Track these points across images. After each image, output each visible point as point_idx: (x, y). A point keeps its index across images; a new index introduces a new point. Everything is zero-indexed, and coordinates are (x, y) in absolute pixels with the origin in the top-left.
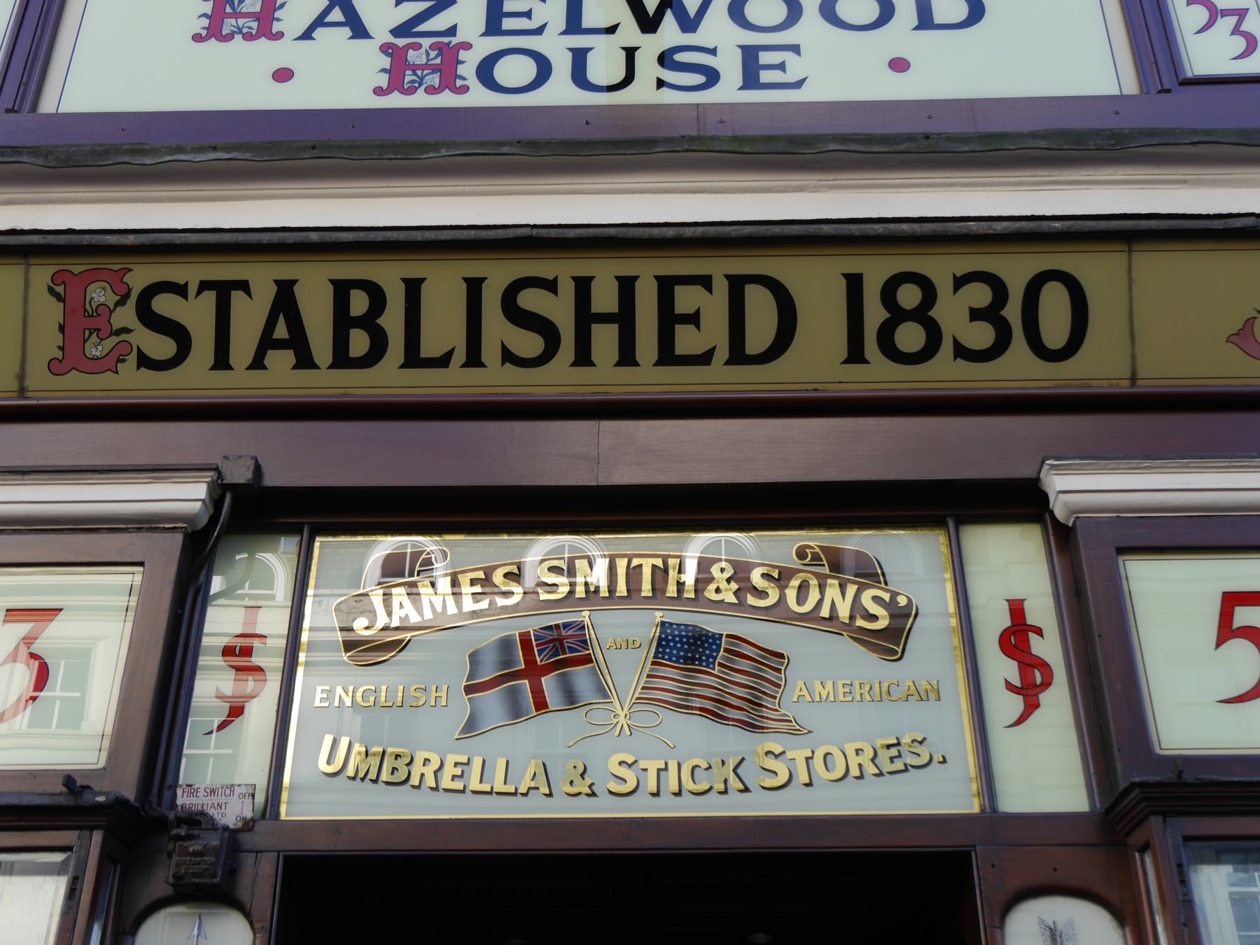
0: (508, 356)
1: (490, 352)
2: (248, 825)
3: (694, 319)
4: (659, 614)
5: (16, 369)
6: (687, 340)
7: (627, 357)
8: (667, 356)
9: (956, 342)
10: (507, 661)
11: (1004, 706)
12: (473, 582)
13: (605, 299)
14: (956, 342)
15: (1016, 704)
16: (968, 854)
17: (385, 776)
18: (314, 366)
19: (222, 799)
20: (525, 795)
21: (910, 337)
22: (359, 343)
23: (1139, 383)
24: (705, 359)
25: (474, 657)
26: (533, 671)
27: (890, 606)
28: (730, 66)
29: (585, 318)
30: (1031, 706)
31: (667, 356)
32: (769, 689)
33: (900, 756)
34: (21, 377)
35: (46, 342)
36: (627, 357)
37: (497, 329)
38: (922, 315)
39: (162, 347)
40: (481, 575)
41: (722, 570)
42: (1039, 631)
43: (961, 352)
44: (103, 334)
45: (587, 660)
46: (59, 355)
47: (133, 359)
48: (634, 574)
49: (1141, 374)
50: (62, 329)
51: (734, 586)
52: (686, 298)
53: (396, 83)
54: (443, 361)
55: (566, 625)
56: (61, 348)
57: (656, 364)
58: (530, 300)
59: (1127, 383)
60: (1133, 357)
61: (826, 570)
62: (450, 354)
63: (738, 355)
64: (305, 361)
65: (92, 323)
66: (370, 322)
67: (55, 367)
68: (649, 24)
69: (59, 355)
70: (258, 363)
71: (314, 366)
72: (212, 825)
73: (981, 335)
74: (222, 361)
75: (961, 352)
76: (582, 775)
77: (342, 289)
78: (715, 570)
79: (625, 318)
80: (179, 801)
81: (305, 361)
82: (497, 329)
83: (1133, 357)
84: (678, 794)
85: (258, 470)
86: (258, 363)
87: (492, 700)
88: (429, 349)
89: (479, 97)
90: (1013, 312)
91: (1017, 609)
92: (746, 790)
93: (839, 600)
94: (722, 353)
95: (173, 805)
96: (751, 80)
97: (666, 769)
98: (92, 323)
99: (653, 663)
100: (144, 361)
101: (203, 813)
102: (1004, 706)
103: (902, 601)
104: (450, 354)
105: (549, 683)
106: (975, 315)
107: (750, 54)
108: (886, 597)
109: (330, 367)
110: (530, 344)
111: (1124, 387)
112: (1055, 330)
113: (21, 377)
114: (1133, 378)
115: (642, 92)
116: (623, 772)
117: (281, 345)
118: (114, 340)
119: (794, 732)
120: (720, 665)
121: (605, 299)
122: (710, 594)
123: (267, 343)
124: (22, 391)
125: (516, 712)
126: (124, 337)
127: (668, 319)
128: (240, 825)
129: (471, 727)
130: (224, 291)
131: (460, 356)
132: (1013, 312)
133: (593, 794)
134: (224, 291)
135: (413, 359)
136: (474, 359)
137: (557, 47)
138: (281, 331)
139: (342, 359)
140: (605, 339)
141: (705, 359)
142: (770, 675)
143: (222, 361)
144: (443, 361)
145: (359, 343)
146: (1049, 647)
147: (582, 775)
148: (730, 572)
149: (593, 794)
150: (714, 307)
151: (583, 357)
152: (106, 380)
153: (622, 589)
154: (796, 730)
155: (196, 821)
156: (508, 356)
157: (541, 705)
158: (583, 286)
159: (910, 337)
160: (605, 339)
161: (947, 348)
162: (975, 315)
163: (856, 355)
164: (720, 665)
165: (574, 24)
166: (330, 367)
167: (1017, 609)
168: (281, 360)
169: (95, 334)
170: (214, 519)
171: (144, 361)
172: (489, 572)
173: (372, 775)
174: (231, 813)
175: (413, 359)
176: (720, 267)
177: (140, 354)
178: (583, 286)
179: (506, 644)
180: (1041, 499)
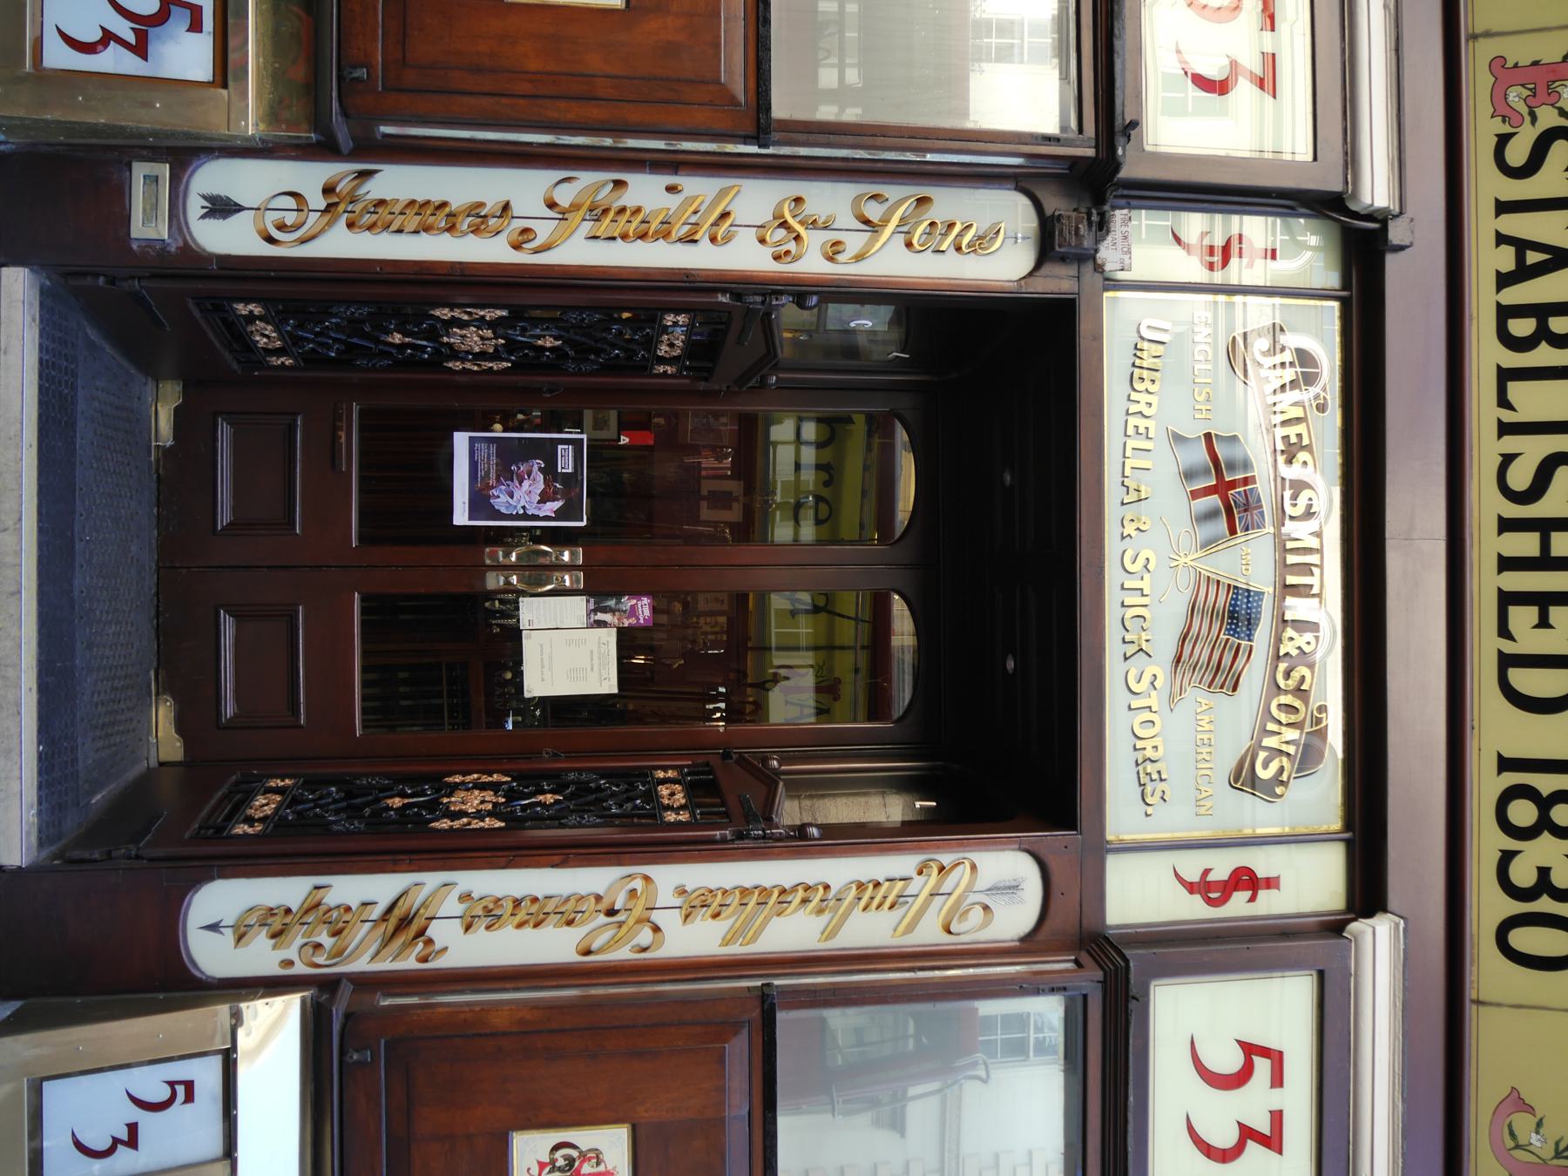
0: (1508, 459)
1: (1512, 443)
2: (1099, 268)
3: (1544, 623)
4: (1271, 590)
5: (1495, 29)
6: (1523, 617)
7: (1507, 564)
8: (1507, 599)
9: (1516, 853)
10: (1232, 466)
11: (1192, 865)
12: (1299, 436)
14: (1516, 853)
15: (1194, 876)
16: (1075, 829)
17: (1137, 371)
18: (1499, 289)
19: (1119, 246)
20: (1123, 484)
21: (1523, 813)
22: (1522, 327)
23: (1474, 1007)
24: (1504, 632)
25: (1234, 438)
26: (1222, 488)
27: (1278, 780)
30: (1191, 888)
31: (1507, 599)
32: (1207, 678)
33: (1152, 780)
34: (1488, 34)
35: (1521, 52)
36: (1507, 564)
37: (1535, 449)
39: (1517, 154)
40: (1305, 442)
41: (1308, 643)
42: (1252, 899)
43: (1507, 857)
44: (1531, 101)
45: (1233, 531)
46: (1510, 64)
47: (1507, 129)
48: (1306, 569)
49: (1482, 1009)
50: (1535, 63)
51: (1294, 652)
54: (1504, 402)
55: (1262, 514)
56: (1516, 66)
57: (1500, 590)
59: (1474, 996)
60: (1499, 1005)
61: (1308, 729)
62: (1510, 407)
63: (1507, 661)
64: (1504, 281)
65: (1541, 91)
66: (1543, 335)
67: (1498, 63)
69: (1510, 64)
70: (1501, 239)
71: (1499, 289)
72: (1098, 241)
73: (1523, 874)
74: (1503, 208)
75: (1507, 857)
76: (1138, 529)
78: (1309, 636)
80: (1117, 212)
81: (1504, 281)
82: (1535, 449)
83: (1499, 1005)
84: (1123, 605)
85: (1401, 248)
86: (1501, 239)
87: (1200, 455)
88: (1515, 389)
90: (1545, 904)
91: (1271, 883)
92: (1126, 659)
94: (1509, 647)
95: (1114, 208)
97: (1143, 595)
98: (1541, 91)
99: (1229, 585)
100: (1503, 140)
101: (1108, 232)
103: (1279, 790)
104: (1510, 407)
105: (1214, 500)
106: (1544, 872)
108: (1284, 777)
109: (1498, 304)
110: (1520, 477)
111: (1471, 993)
112: (1521, 939)
113: (1488, 34)
114: (1478, 1002)
116: (1141, 561)
117: (1520, 258)
118: (1524, 110)
119: (1171, 697)
120: (1228, 640)
122: (1290, 632)
123: (1521, 246)
124: (1474, 37)
125: (1189, 475)
126: (1528, 119)
128: (1099, 261)
129: (1178, 439)
131: (1508, 417)
132: (1545, 904)
133: (1123, 538)
135: (1506, 376)
136: (1505, 429)
138: (1533, 257)
139: (1505, 313)
140: (1527, 545)
141: (1504, 632)
142: (1219, 680)
143: (1503, 208)
144: (1504, 402)
145: (1522, 327)
146: (1239, 906)
147: (1138, 529)
148: (1307, 649)
149: (1123, 538)
151: (1506, 525)
152: (1485, 108)
153: (1292, 559)
154: (1172, 700)
155: (1102, 227)
156: (1508, 459)
157: (1195, 495)
159: (1523, 813)
160: (1527, 545)
161: (1511, 844)
162: (1544, 872)
163: (1506, 764)
164: (1228, 640)
166: (1498, 304)
167: (1271, 883)
168: (1506, 259)
169: (1529, 93)
170: (1356, 215)
171: (1503, 140)
172: (1309, 448)
173: (1138, 362)
174: (1108, 254)
175: (1506, 376)
177: (1511, 136)
179: (1247, 465)
180: (1368, 913)
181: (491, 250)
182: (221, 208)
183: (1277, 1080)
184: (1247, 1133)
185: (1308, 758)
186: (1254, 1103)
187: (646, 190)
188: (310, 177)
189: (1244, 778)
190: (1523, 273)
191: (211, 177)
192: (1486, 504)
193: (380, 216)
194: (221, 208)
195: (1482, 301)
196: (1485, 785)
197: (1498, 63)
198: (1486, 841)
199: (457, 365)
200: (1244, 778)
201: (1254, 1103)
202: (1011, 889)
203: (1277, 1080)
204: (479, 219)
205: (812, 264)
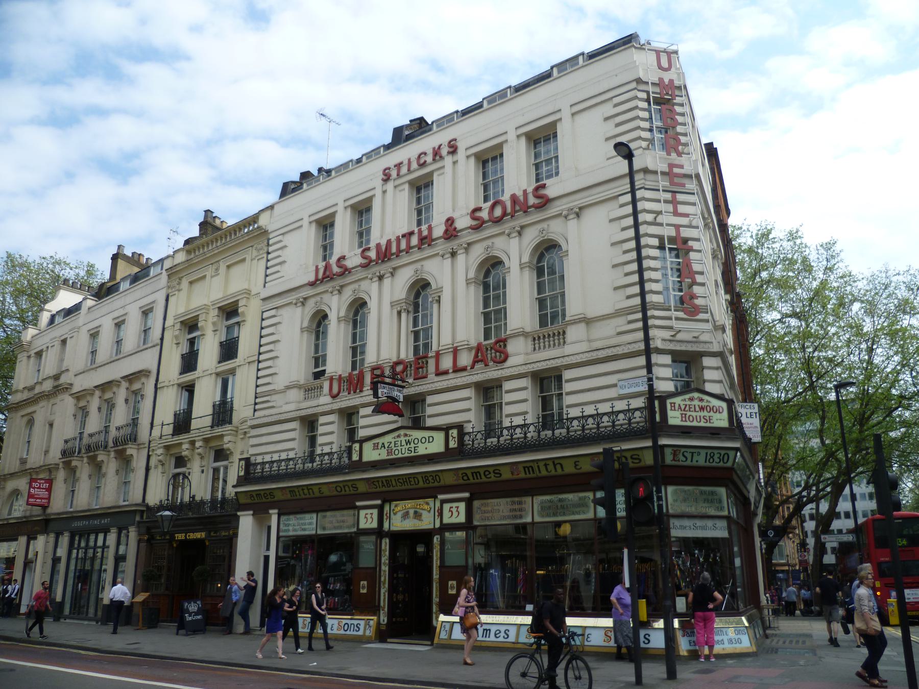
6: (412, 483)
13: (405, 480)
28: (413, 450)
29: (404, 482)
37: (398, 484)
38: (428, 479)
52: (410, 479)
53: (388, 455)
58: (400, 480)
63: (416, 484)
68: (407, 445)
77: (386, 481)
79: (406, 482)
89: (394, 456)
93: (426, 507)
96: (415, 452)
102: (436, 517)
107: (415, 447)
115: (406, 455)
121: (405, 480)
127: (410, 482)
130: (378, 481)
134: (378, 481)
137: (399, 448)
150: (412, 480)
158: (403, 479)
159: (428, 482)
165: (401, 446)
176: (412, 476)
178: (403, 479)
181: (387, 594)
182: (384, 621)
183: (452, 507)
184: (457, 511)
185: (427, 504)
186: (454, 510)
187: (382, 579)
188: (382, 612)
189: (429, 511)
190: (384, 486)
191: (381, 622)
192: (404, 487)
193: (384, 605)
194: (384, 621)
195: (387, 489)
196: (426, 485)
197: (369, 488)
198: (431, 485)
199: (407, 600)
200: (429, 511)
201: (454, 510)
202: (437, 538)
203: (452, 507)
204: (384, 596)
205: (387, 562)
